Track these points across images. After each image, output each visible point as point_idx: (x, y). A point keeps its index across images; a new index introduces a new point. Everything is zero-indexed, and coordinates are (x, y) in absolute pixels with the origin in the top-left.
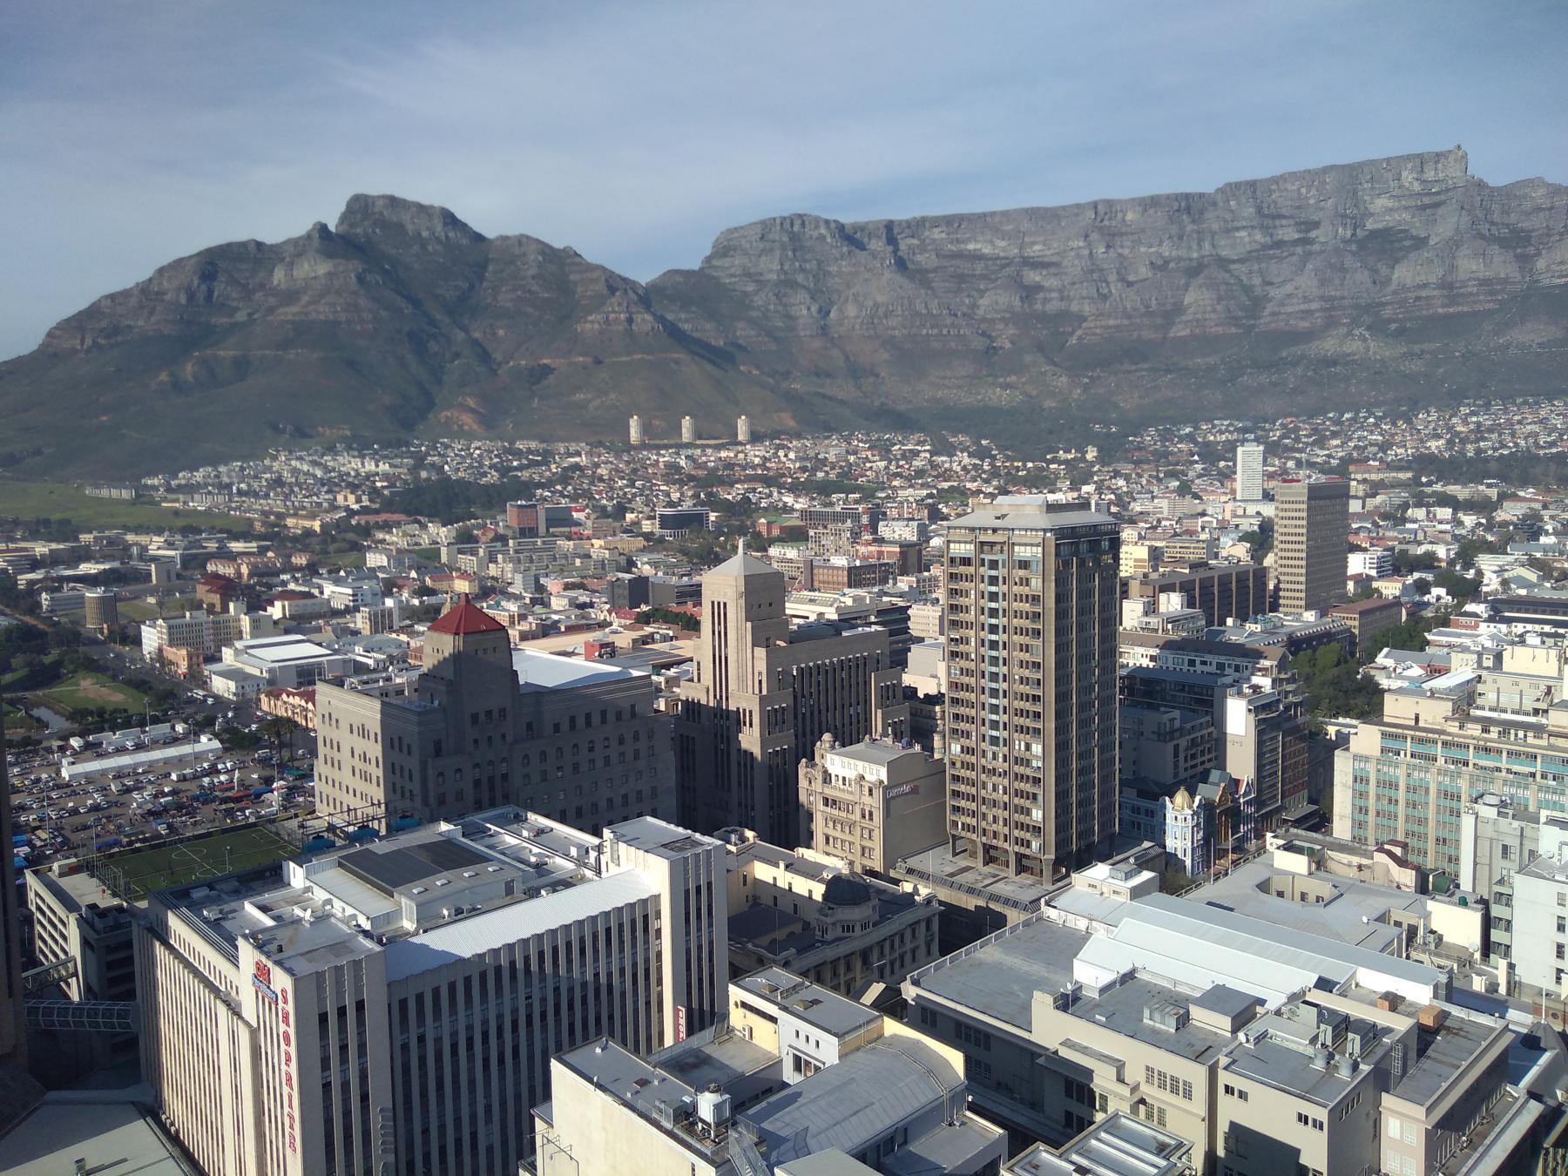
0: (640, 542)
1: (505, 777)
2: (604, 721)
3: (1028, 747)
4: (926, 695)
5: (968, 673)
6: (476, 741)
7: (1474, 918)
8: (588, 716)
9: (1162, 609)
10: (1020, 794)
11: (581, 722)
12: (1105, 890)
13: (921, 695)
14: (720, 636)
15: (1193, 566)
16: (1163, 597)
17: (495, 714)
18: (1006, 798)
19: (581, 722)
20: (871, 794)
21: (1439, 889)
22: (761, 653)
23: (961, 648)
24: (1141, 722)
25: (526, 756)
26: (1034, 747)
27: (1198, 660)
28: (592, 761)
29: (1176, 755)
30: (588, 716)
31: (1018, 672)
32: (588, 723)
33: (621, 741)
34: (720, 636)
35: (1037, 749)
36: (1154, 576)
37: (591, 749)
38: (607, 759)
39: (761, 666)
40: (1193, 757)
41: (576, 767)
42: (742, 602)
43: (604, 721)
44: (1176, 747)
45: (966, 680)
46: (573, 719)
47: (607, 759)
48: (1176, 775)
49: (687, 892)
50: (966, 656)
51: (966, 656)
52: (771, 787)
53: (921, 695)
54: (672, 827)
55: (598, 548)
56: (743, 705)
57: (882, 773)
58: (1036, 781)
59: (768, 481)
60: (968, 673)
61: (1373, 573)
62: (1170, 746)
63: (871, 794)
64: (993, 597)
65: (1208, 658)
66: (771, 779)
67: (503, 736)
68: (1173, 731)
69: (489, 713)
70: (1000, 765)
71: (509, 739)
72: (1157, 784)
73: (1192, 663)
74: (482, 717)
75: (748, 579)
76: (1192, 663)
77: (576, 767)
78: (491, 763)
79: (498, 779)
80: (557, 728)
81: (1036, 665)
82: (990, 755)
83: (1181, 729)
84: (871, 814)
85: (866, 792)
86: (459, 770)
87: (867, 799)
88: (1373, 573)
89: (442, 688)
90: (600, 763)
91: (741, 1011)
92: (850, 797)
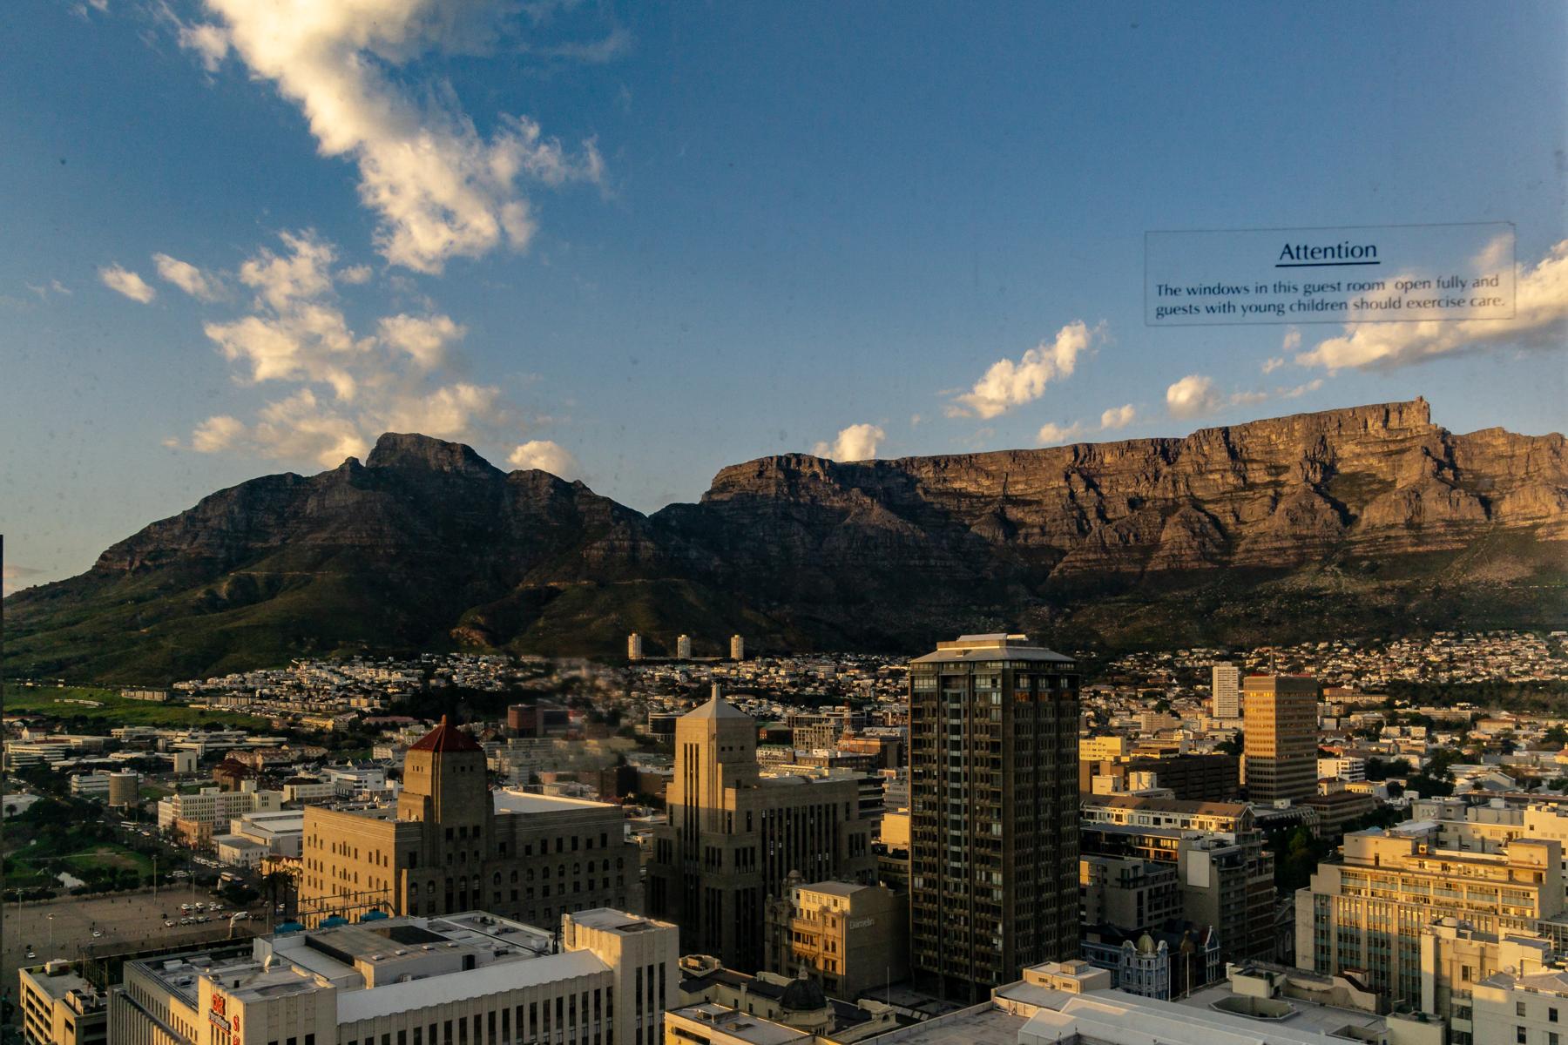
0: (632, 743)
1: (477, 894)
2: (575, 847)
3: (989, 877)
4: (895, 851)
5: (932, 806)
6: (450, 856)
8: (560, 841)
9: (1133, 787)
10: (983, 924)
11: (552, 847)
12: (1056, 983)
13: (890, 851)
14: (692, 776)
15: (1163, 752)
16: (1133, 776)
17: (470, 832)
18: (967, 929)
19: (552, 847)
20: (834, 925)
22: (731, 793)
23: (925, 781)
24: (1105, 869)
25: (498, 875)
26: (995, 876)
27: (1163, 818)
28: (562, 886)
29: (1140, 902)
30: (560, 841)
31: (980, 803)
32: (560, 848)
33: (591, 868)
34: (692, 776)
35: (997, 878)
36: (1125, 759)
37: (561, 874)
38: (577, 886)
39: (731, 805)
40: (1158, 907)
41: (546, 892)
42: (714, 743)
43: (575, 847)
44: (1140, 895)
45: (929, 813)
46: (544, 843)
47: (577, 886)
48: (1140, 922)
49: (639, 971)
50: (930, 790)
51: (930, 790)
52: (738, 926)
53: (890, 851)
54: (629, 915)
55: (593, 746)
56: (713, 844)
57: (845, 904)
58: (995, 910)
60: (932, 806)
61: (1346, 777)
62: (1133, 894)
63: (834, 925)
64: (956, 730)
65: (1173, 816)
66: (738, 917)
67: (477, 854)
68: (1136, 879)
69: (463, 830)
70: (961, 894)
71: (482, 855)
72: (1122, 931)
73: (1157, 821)
74: (456, 833)
75: (720, 722)
76: (1157, 821)
77: (546, 892)
78: (464, 879)
79: (470, 894)
80: (528, 850)
81: (995, 795)
82: (952, 887)
83: (1144, 877)
84: (834, 945)
85: (830, 923)
86: (431, 883)
87: (830, 931)
88: (1346, 777)
89: (421, 803)
90: (569, 889)
91: (676, 1038)
92: (815, 930)
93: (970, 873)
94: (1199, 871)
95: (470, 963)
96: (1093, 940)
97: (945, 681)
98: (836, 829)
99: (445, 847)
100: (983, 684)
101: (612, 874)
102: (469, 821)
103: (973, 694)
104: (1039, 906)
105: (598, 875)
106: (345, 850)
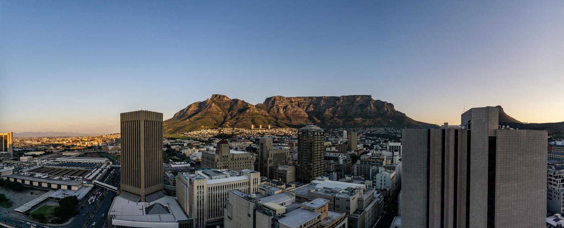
7: (372, 182)
21: (367, 179)
59: (273, 134)
93: (307, 163)
94: (341, 162)
95: (226, 177)
96: (326, 173)
97: (304, 133)
98: (286, 157)
99: (223, 159)
100: (310, 133)
101: (249, 164)
102: (226, 155)
103: (308, 135)
104: (318, 168)
105: (247, 164)
106: (208, 159)
